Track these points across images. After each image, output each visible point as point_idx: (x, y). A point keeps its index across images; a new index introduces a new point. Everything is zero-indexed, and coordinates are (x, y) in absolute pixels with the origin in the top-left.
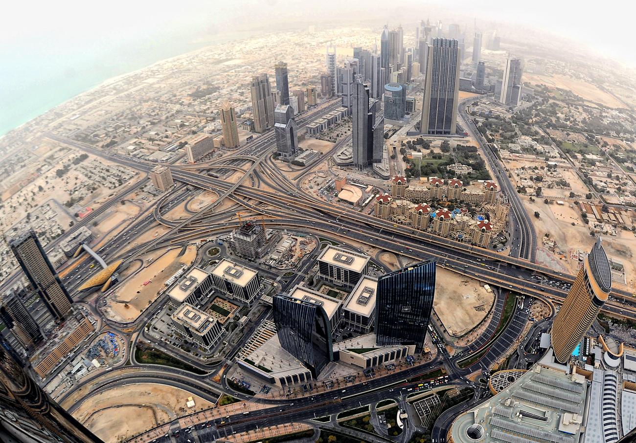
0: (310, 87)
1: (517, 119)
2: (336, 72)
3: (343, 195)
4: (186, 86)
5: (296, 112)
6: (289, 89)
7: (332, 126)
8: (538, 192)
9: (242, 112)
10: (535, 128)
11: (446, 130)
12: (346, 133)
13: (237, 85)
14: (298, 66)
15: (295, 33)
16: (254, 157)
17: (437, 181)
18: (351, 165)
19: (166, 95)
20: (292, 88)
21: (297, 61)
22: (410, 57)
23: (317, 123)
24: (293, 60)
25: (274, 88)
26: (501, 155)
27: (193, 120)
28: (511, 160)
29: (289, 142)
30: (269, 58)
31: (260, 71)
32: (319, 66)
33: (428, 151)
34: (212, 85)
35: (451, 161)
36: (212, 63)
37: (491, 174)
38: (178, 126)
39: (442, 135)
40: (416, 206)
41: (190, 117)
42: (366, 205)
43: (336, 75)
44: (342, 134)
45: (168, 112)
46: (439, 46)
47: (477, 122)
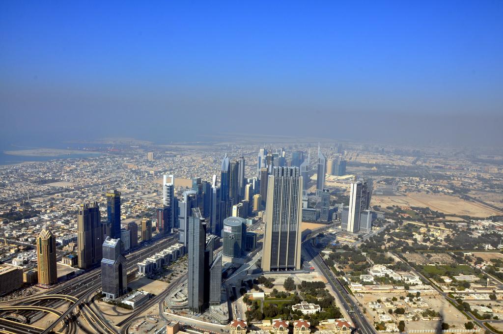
0: (144, 220)
1: (366, 247)
2: (173, 205)
6: (121, 222)
9: (66, 243)
10: (389, 254)
11: (290, 266)
12: (181, 272)
14: (133, 196)
15: (132, 158)
16: (73, 297)
17: (281, 323)
18: (185, 308)
21: (133, 190)
24: (129, 188)
25: (105, 218)
30: (102, 184)
32: (156, 198)
33: (271, 290)
34: (32, 208)
36: (35, 182)
37: (343, 311)
39: (285, 272)
44: (178, 274)
46: (280, 175)
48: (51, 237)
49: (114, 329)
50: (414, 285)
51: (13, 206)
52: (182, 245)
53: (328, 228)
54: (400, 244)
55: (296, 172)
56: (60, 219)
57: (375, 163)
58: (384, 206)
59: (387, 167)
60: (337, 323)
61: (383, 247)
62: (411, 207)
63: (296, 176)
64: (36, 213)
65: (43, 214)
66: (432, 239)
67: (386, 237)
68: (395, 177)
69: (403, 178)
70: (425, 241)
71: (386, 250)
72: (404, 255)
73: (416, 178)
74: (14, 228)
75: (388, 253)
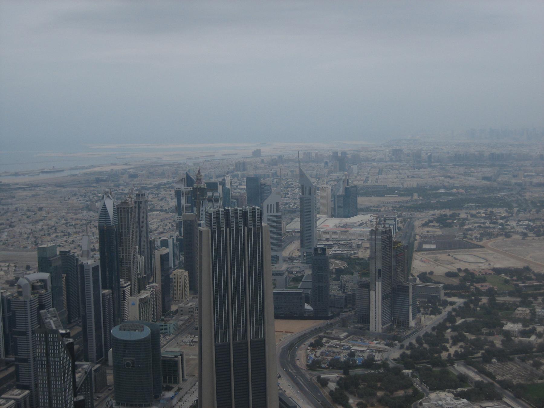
10: (460, 369)
22: (164, 258)
46: (223, 226)
47: (324, 383)
52: (27, 392)
53: (331, 326)
54: (477, 345)
57: (415, 186)
58: (440, 270)
59: (442, 191)
61: (444, 355)
62: (495, 270)
63: (254, 225)
68: (457, 212)
69: (474, 212)
70: (525, 334)
71: (451, 361)
72: (488, 367)
73: (500, 210)
75: (455, 365)
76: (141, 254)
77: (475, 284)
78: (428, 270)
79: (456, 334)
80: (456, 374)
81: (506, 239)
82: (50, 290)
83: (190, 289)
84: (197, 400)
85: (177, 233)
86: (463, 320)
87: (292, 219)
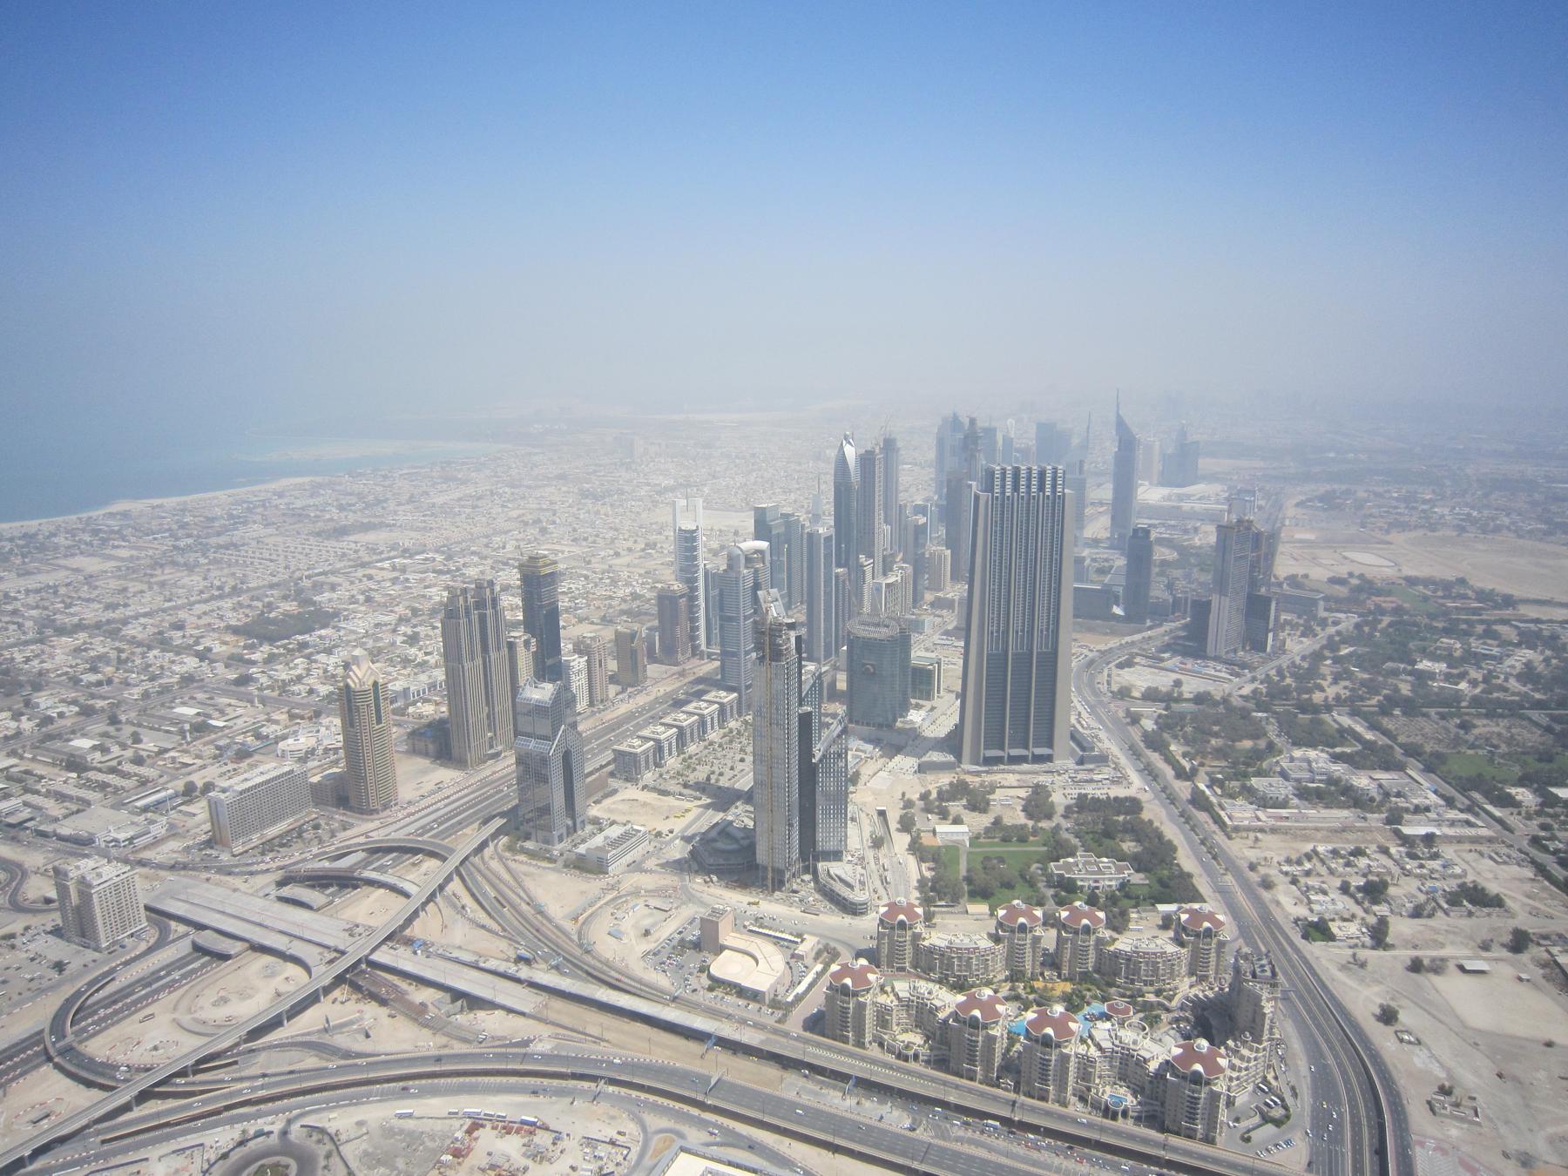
2: (701, 584)
3: (727, 966)
4: (221, 597)
5: (582, 705)
7: (692, 749)
8: (1378, 935)
11: (1038, 751)
13: (401, 610)
17: (1022, 913)
19: (142, 620)
20: (571, 631)
23: (647, 739)
25: (514, 625)
26: (1226, 819)
27: (240, 711)
28: (1262, 830)
29: (558, 800)
31: (472, 572)
34: (314, 603)
35: (1059, 850)
36: (318, 534)
37: (1202, 884)
38: (187, 727)
40: (961, 998)
41: (233, 702)
42: (799, 998)
43: (701, 593)
45: (153, 679)
46: (1008, 492)
47: (1135, 719)
48: (375, 684)
49: (557, 927)
50: (1418, 810)
51: (267, 600)
52: (735, 695)
55: (1054, 479)
56: (394, 631)
59: (1332, 455)
60: (1184, 917)
64: (325, 618)
65: (346, 618)
66: (1475, 674)
67: (1327, 667)
69: (1381, 490)
71: (1328, 708)
72: (1386, 722)
74: (271, 659)
76: (886, 522)
77: (1374, 598)
78: (1300, 571)
79: (1338, 668)
80: (1336, 726)
81: (1429, 534)
82: (768, 565)
83: (952, 579)
84: (956, 725)
85: (936, 497)
86: (1352, 649)
87: (1099, 485)
